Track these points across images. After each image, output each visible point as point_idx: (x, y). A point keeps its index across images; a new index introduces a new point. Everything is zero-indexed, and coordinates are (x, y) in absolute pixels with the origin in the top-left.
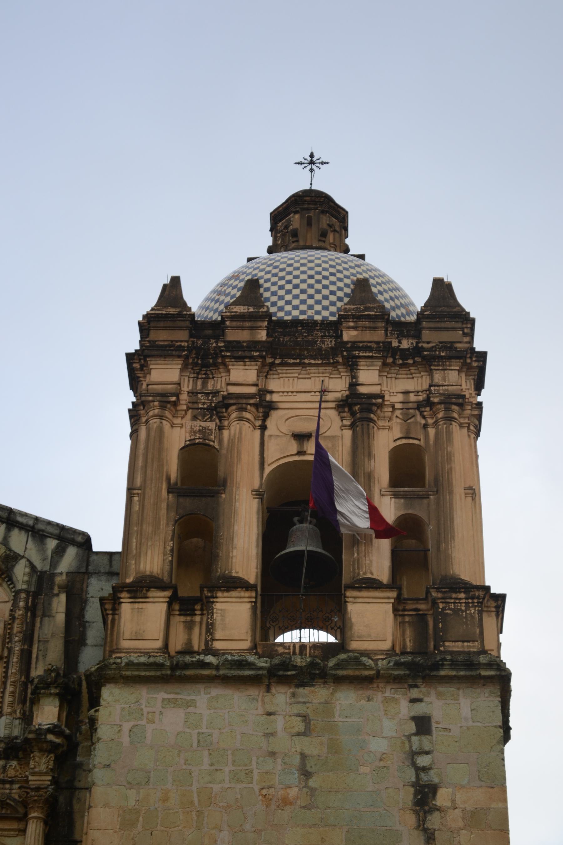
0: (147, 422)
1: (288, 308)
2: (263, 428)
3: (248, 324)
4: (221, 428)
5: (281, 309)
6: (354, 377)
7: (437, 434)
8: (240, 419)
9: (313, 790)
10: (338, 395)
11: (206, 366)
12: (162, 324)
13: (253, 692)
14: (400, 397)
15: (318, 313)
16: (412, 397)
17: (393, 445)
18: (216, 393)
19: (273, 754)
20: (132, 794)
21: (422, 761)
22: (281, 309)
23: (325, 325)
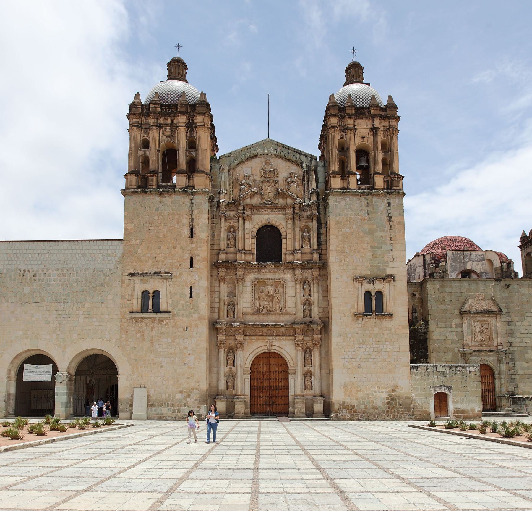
0: (331, 133)
1: (358, 103)
2: (355, 135)
3: (350, 108)
4: (346, 135)
5: (356, 103)
6: (373, 123)
7: (391, 137)
8: (351, 133)
9: (370, 217)
10: (370, 127)
11: (342, 119)
12: (332, 108)
13: (358, 197)
14: (382, 128)
15: (364, 104)
16: (385, 128)
17: (381, 140)
18: (344, 126)
19: (362, 210)
20: (337, 218)
21: (389, 212)
22: (356, 103)
23: (366, 108)
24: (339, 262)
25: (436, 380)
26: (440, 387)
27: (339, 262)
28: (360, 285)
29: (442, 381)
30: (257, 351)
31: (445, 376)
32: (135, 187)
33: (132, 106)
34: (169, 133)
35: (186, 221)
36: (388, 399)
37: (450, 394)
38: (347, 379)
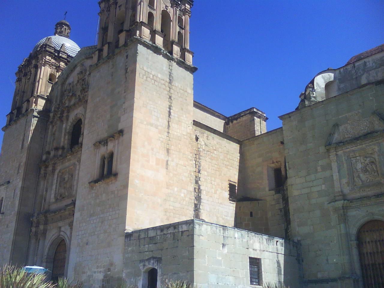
21: (126, 64)
24: (89, 133)
25: (146, 250)
26: (149, 260)
27: (89, 133)
28: (98, 149)
29: (152, 251)
30: (52, 238)
31: (156, 243)
32: (8, 123)
33: (19, 68)
34: (29, 77)
35: (22, 138)
36: (103, 280)
37: (158, 271)
38: (78, 259)
